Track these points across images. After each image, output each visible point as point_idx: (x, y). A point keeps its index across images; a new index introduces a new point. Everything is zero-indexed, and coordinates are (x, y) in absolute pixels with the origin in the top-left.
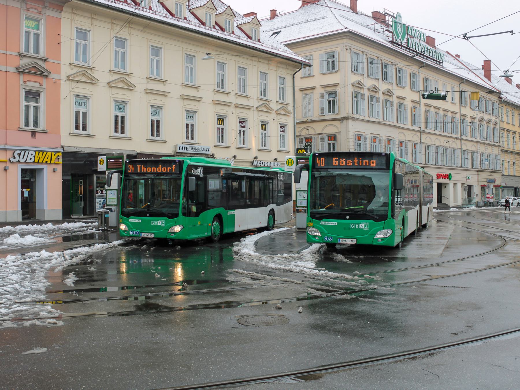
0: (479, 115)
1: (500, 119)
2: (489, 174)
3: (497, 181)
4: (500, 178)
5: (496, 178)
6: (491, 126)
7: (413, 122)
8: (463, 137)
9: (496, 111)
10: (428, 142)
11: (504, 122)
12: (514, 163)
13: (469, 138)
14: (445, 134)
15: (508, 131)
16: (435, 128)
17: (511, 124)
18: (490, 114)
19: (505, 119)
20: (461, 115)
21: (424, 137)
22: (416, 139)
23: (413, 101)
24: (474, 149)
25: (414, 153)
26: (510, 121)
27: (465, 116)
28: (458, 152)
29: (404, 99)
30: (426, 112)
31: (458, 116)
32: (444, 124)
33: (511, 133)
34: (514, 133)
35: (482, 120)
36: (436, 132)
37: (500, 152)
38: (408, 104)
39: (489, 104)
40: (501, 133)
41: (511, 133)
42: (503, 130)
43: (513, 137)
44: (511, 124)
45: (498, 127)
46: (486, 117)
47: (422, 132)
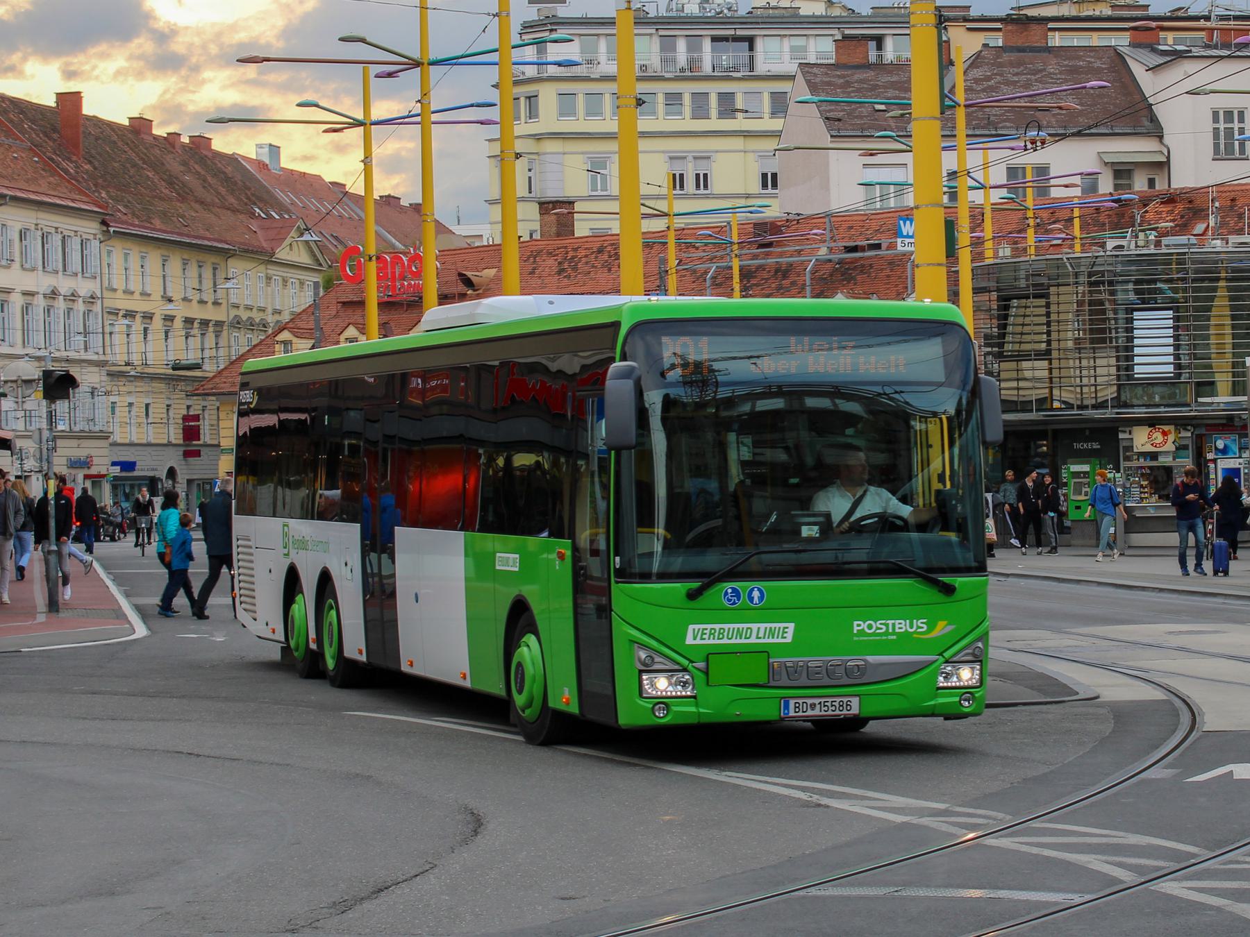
1: (106, 284)
2: (74, 443)
3: (96, 461)
4: (105, 452)
5: (93, 452)
6: (80, 306)
9: (93, 263)
11: (115, 290)
12: (147, 406)
13: (19, 350)
15: (130, 314)
17: (137, 296)
18: (76, 275)
19: (118, 283)
26: (135, 286)
33: (138, 318)
34: (148, 317)
35: (53, 294)
37: (105, 378)
39: (75, 244)
40: (107, 323)
41: (138, 318)
42: (114, 313)
43: (146, 330)
44: (137, 296)
45: (97, 308)
46: (65, 285)
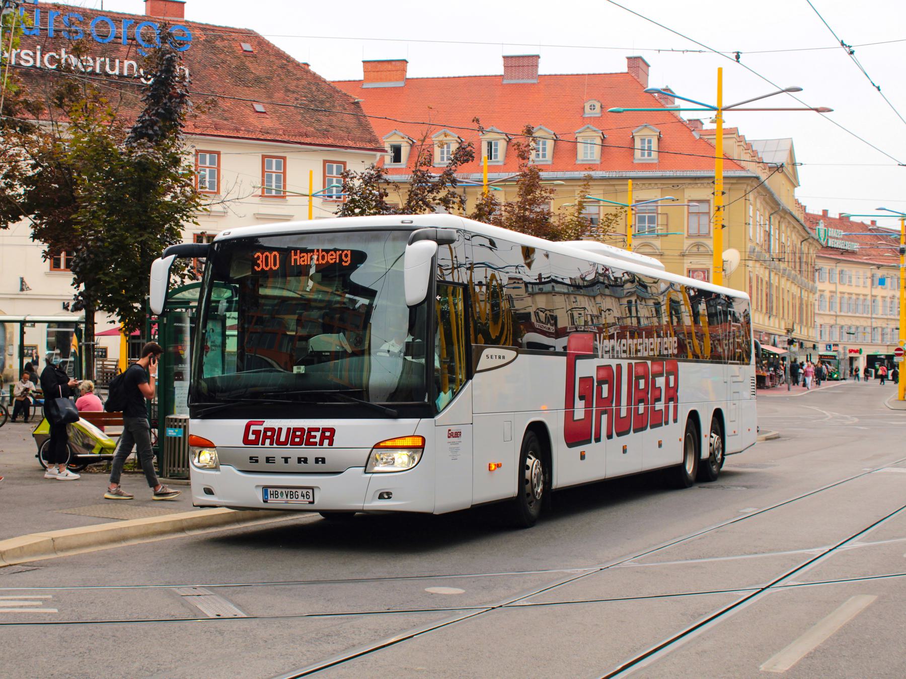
0: (891, 293)
7: (831, 308)
8: (874, 316)
10: (842, 323)
14: (857, 315)
16: (849, 311)
20: (872, 296)
21: (838, 319)
22: (832, 322)
23: (831, 292)
24: (884, 325)
25: (831, 333)
27: (875, 296)
28: (869, 330)
29: (823, 291)
30: (841, 298)
31: (869, 298)
32: (857, 305)
36: (850, 314)
38: (827, 294)
47: (836, 316)
